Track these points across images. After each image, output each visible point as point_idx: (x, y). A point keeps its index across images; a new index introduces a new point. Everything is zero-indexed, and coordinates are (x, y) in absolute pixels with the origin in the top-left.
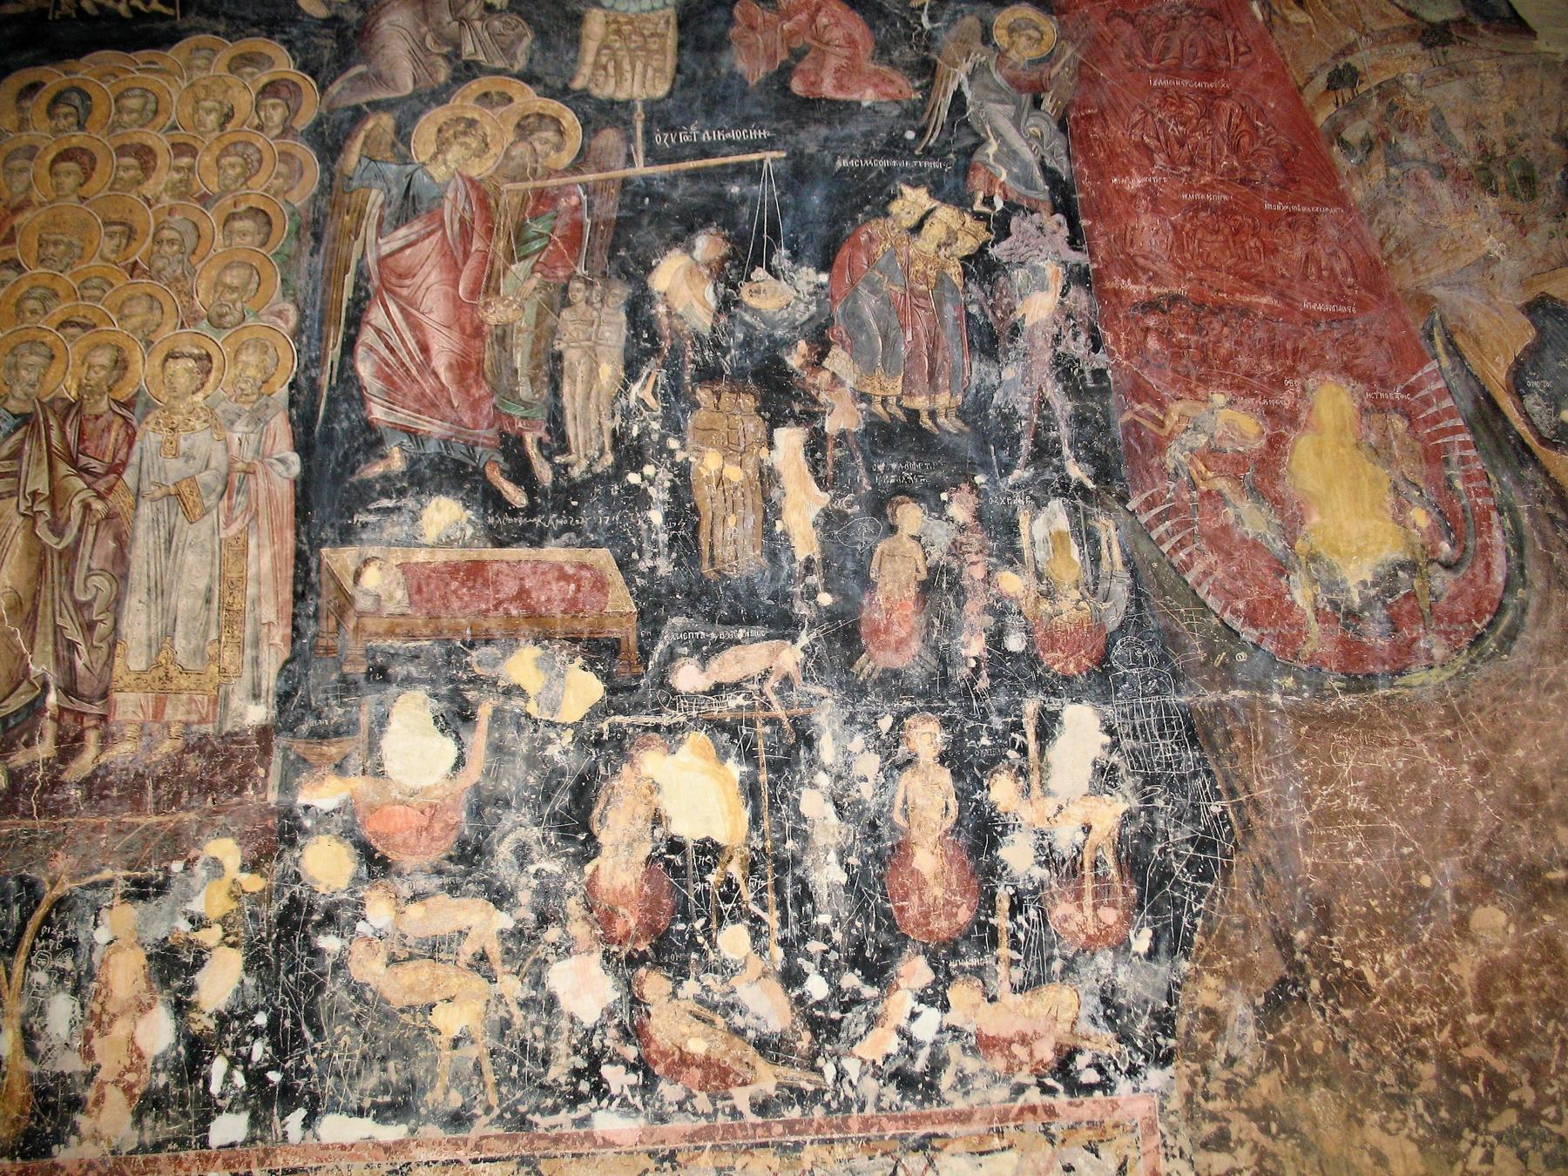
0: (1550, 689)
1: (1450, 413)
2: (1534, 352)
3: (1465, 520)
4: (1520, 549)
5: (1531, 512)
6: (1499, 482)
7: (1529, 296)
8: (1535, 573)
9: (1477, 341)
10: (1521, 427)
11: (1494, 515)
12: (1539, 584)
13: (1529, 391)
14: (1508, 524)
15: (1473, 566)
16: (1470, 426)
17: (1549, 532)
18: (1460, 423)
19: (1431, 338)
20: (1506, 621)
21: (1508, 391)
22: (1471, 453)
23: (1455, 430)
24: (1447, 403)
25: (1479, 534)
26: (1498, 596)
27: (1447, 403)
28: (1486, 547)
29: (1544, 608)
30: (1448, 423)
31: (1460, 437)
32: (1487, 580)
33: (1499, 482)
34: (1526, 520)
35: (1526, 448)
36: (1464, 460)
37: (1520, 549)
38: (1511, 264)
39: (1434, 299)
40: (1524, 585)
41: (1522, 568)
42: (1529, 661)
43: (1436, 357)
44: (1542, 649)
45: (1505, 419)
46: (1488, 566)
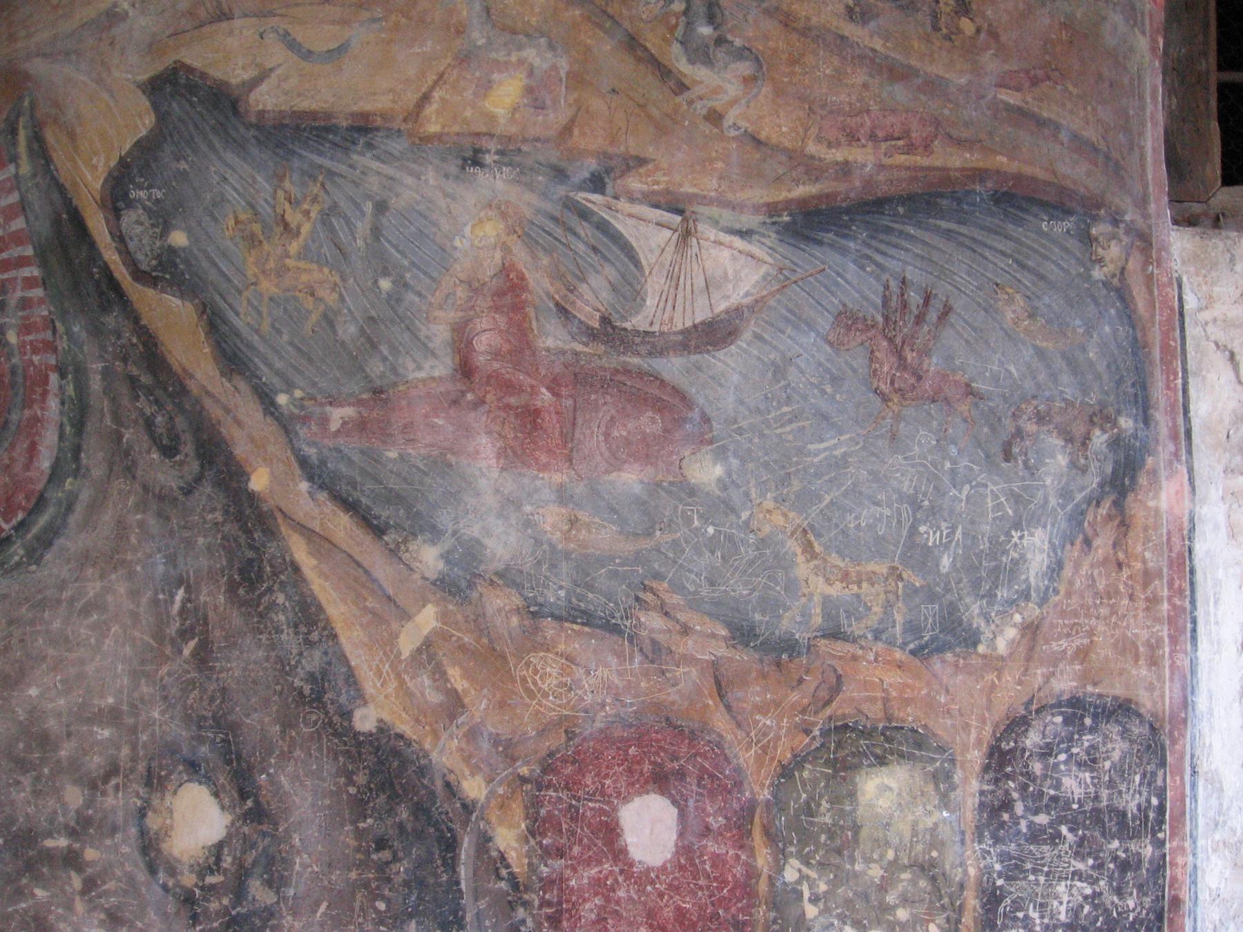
0: (86, 611)
1: (18, 238)
2: (147, 149)
3: (13, 385)
4: (79, 426)
5: (106, 373)
6: (68, 332)
7: (157, 68)
8: (95, 459)
9: (72, 136)
10: (111, 256)
11: (54, 378)
12: (98, 472)
13: (130, 204)
14: (70, 390)
15: (13, 446)
16: (42, 258)
17: (125, 401)
18: (29, 251)
19: (14, 132)
20: (43, 520)
21: (102, 205)
22: (38, 292)
23: (22, 262)
24: (19, 224)
25: (28, 403)
26: (40, 486)
27: (19, 224)
28: (36, 421)
29: (95, 506)
30: (16, 252)
31: (27, 272)
32: (27, 467)
33: (68, 332)
34: (96, 384)
35: (115, 286)
36: (25, 304)
37: (79, 426)
38: (143, 21)
39: (27, 77)
40: (76, 474)
41: (77, 450)
42: (65, 574)
43: (14, 159)
44: (85, 558)
45: (92, 245)
46: (32, 450)
